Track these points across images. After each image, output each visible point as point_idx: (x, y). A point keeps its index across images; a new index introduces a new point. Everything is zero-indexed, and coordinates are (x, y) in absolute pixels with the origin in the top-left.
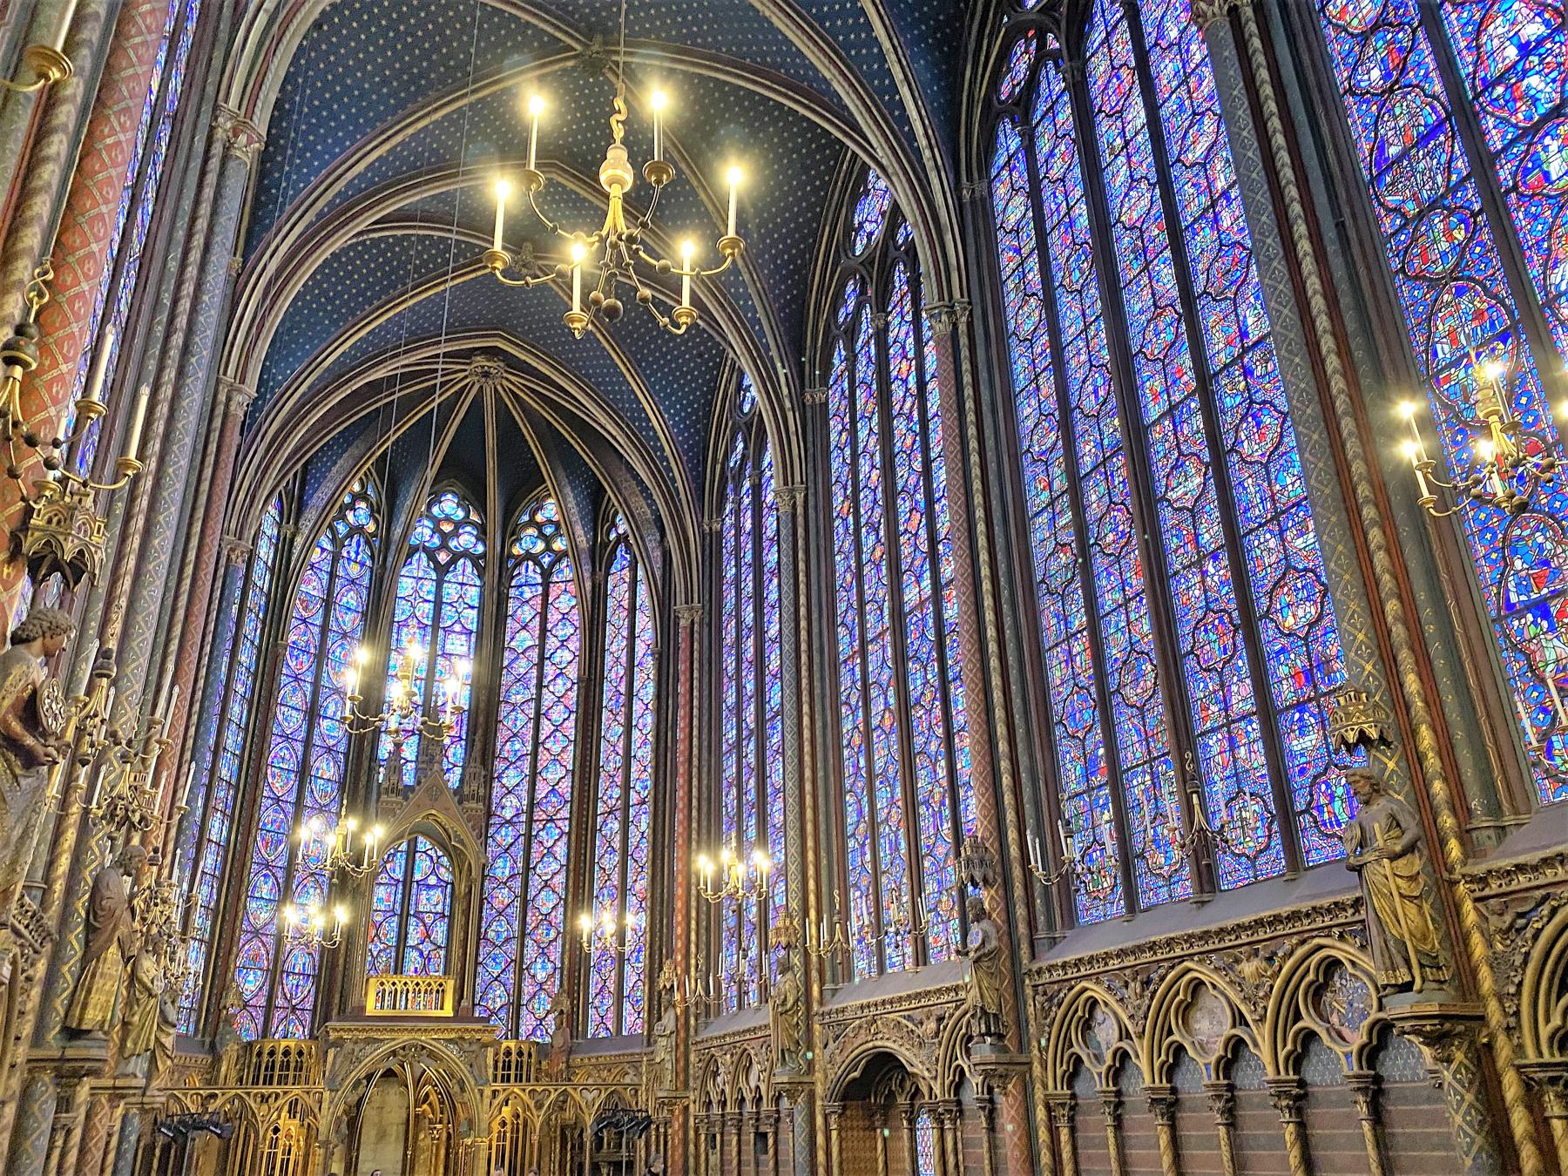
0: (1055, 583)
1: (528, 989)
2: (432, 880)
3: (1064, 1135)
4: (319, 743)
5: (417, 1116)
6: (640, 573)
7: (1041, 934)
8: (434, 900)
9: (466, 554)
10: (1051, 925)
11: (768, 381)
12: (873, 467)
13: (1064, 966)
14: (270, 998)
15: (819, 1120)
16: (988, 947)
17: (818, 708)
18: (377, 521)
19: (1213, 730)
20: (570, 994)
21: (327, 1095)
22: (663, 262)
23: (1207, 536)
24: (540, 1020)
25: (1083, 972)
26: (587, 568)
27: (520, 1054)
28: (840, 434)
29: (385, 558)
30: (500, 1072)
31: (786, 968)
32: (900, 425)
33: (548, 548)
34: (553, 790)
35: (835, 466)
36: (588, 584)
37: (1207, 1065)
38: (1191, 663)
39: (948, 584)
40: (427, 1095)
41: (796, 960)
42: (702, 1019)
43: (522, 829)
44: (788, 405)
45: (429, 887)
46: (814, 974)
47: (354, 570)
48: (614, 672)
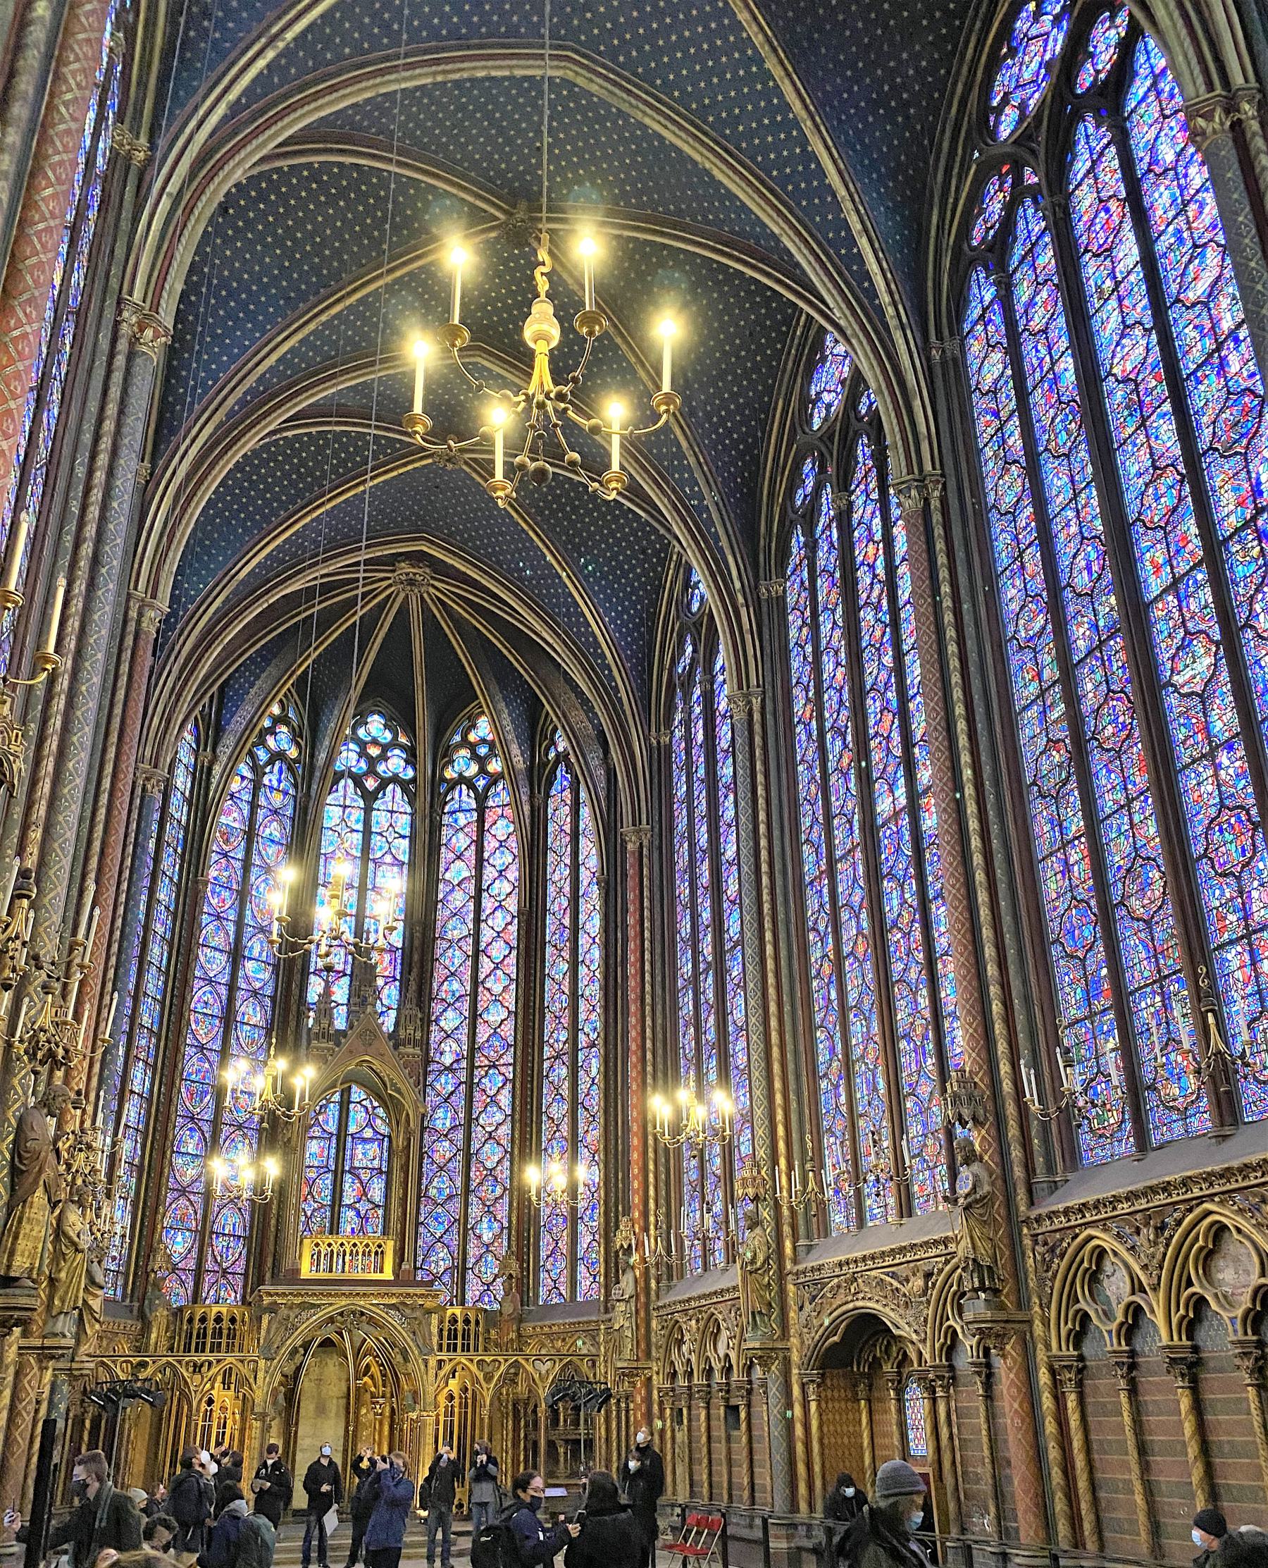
0: (1049, 785)
1: (473, 1251)
2: (368, 1133)
3: (1072, 1401)
4: (244, 986)
5: (358, 1389)
6: (583, 795)
7: (1041, 1177)
8: (371, 1154)
9: (395, 779)
10: (1050, 1169)
11: (718, 574)
12: (838, 664)
13: (1066, 1212)
15: (796, 1391)
16: (980, 1193)
17: (782, 935)
19: (1231, 942)
20: (520, 1260)
21: (262, 1363)
22: (593, 421)
23: (1219, 724)
24: (487, 1285)
25: (1089, 1218)
26: (525, 790)
27: (467, 1321)
28: (800, 629)
29: (309, 787)
30: (445, 1342)
31: (754, 1223)
32: (867, 615)
33: (483, 770)
35: (795, 665)
36: (527, 808)
37: (1232, 1320)
38: (1205, 866)
39: (925, 792)
40: (368, 1366)
41: (765, 1214)
42: (664, 1283)
43: (463, 1076)
44: (741, 599)
45: (365, 1141)
46: (786, 1229)
47: (277, 799)
48: (557, 903)
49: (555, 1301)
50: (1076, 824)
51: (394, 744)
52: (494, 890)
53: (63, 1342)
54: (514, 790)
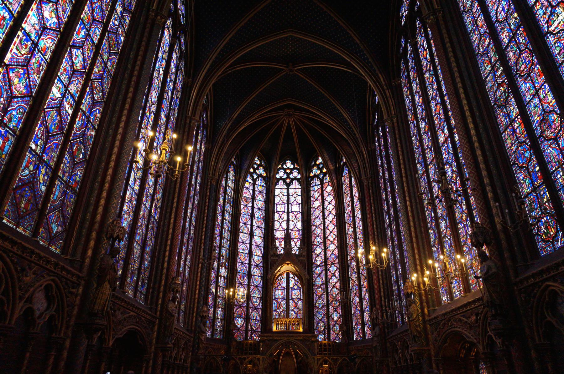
1: (332, 323)
2: (296, 287)
8: (297, 294)
9: (295, 178)
11: (377, 82)
12: (420, 97)
14: (247, 327)
18: (266, 172)
24: (336, 335)
32: (427, 75)
33: (321, 172)
34: (332, 253)
35: (407, 105)
36: (335, 181)
44: (385, 87)
48: (348, 210)
49: (359, 339)
50: (514, 111)
51: (294, 168)
52: (328, 208)
53: (168, 345)
54: (330, 176)
